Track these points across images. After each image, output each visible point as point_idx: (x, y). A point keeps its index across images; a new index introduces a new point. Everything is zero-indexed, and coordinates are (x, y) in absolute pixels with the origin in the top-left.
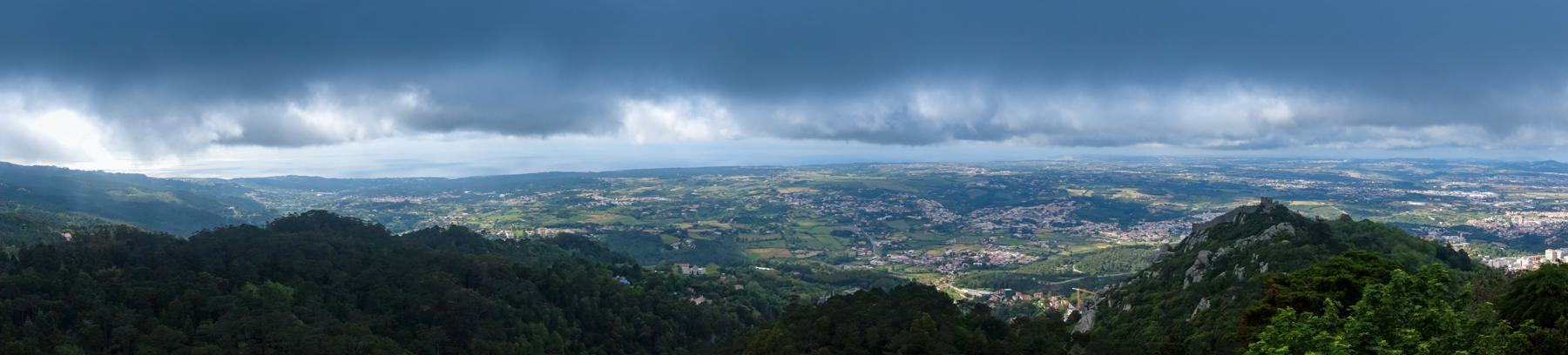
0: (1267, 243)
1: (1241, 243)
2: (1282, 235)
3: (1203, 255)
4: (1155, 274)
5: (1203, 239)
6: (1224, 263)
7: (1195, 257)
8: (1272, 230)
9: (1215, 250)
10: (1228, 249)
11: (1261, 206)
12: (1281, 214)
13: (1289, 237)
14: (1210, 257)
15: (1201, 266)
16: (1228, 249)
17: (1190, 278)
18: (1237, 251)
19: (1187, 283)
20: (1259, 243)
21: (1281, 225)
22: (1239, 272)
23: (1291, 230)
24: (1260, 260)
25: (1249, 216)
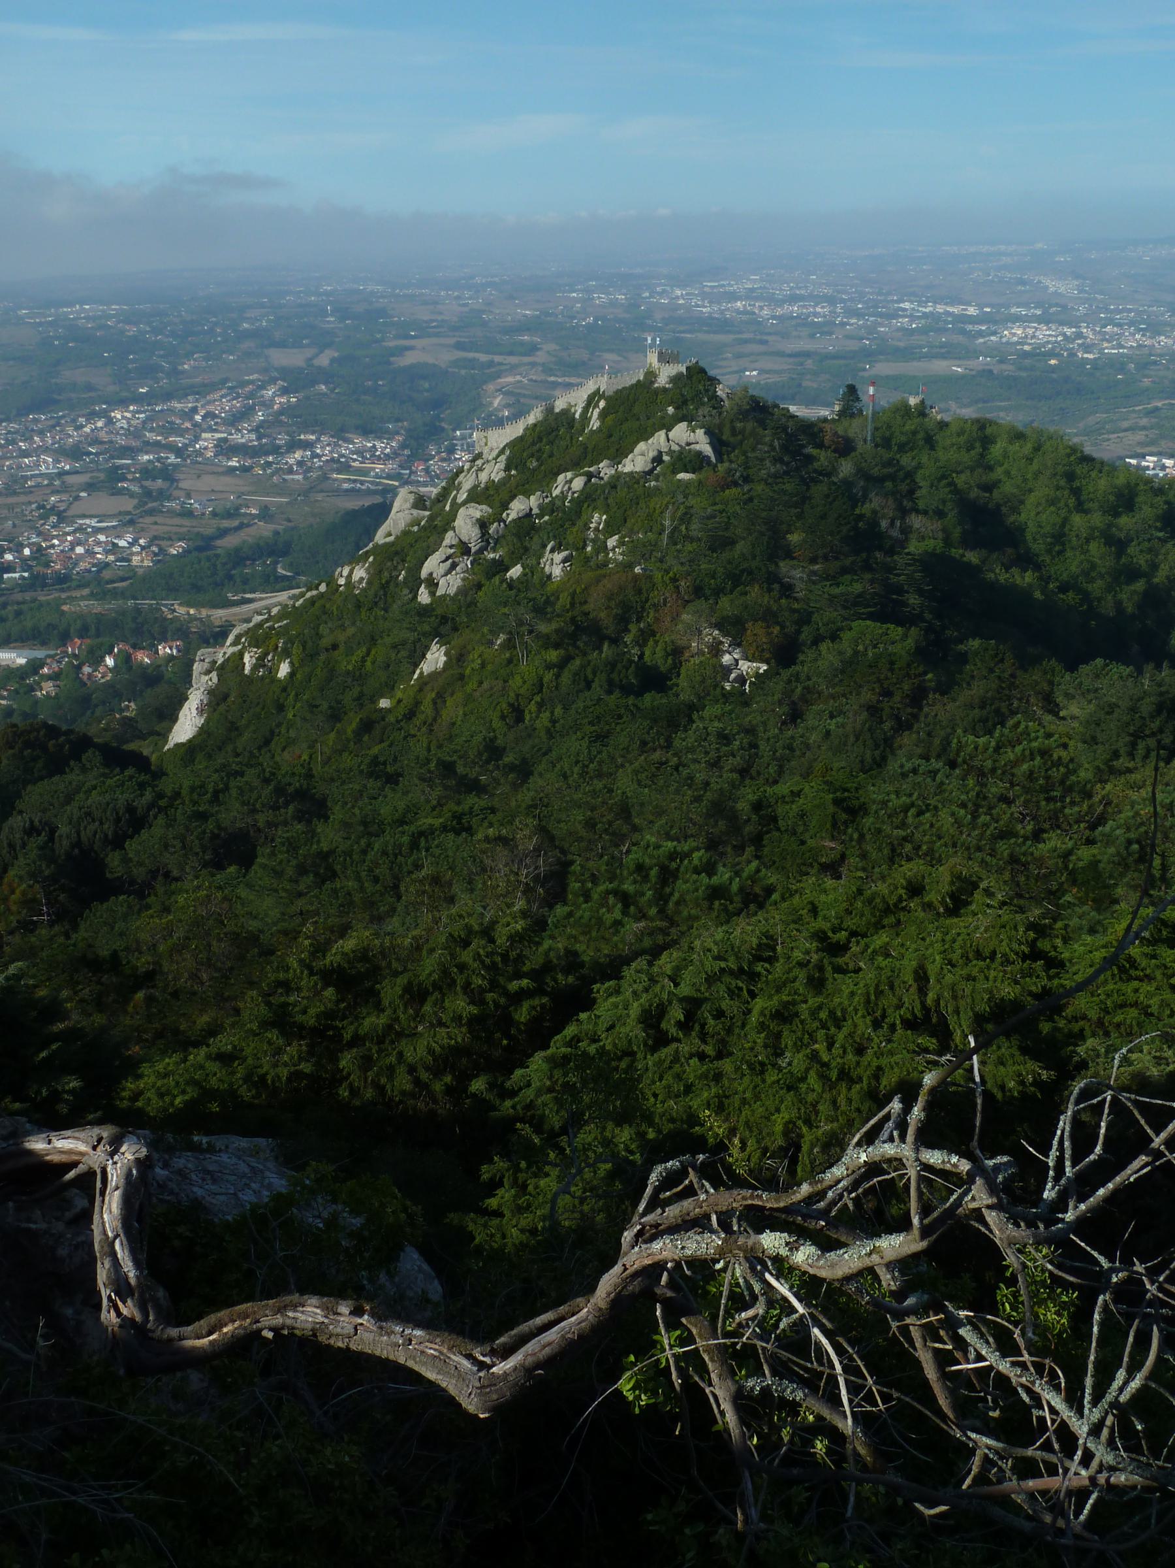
0: (635, 479)
2: (687, 460)
4: (360, 573)
7: (449, 524)
9: (505, 506)
13: (695, 462)
14: (483, 524)
17: (432, 584)
19: (424, 597)
20: (614, 483)
21: (680, 432)
22: (555, 565)
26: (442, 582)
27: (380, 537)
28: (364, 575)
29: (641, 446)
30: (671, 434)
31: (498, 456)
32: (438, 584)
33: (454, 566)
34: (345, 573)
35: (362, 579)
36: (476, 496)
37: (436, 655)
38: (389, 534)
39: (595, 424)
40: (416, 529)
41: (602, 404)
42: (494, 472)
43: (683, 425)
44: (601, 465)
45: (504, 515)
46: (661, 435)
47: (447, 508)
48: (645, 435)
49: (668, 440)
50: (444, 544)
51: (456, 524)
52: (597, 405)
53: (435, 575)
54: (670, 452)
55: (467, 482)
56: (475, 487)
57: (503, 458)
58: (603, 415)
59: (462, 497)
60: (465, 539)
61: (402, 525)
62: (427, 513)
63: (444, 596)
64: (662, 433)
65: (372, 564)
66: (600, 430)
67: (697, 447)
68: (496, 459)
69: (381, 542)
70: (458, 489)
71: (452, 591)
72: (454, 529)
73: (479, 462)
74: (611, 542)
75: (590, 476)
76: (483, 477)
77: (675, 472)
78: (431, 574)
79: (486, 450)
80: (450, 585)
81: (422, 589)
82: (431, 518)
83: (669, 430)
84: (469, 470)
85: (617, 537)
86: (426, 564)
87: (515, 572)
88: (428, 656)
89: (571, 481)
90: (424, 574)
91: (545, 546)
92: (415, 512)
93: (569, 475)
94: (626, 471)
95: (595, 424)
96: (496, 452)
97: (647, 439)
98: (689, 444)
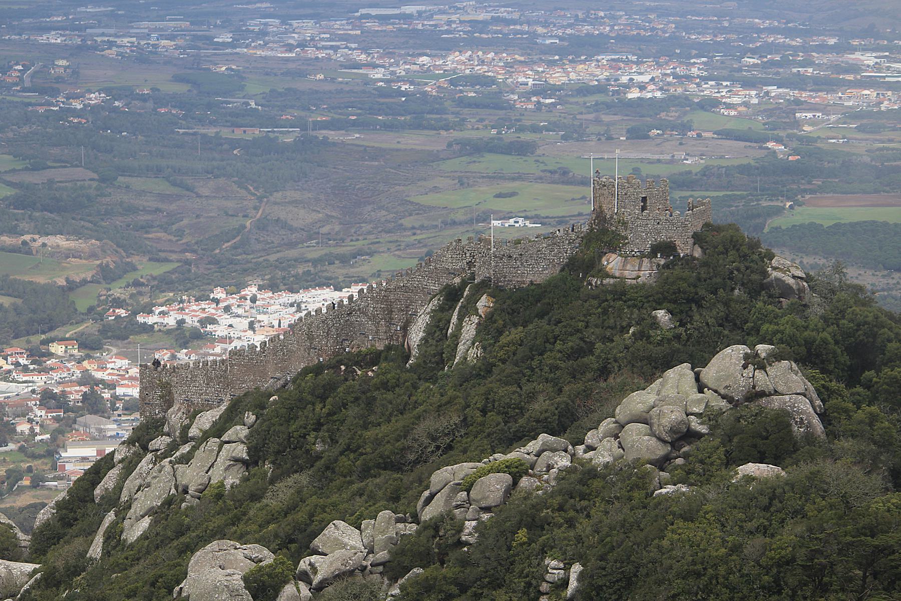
5: (218, 466)
9: (297, 541)
10: (385, 527)
16: (385, 527)
23: (791, 389)
30: (709, 373)
31: (218, 430)
41: (484, 303)
43: (733, 354)
46: (679, 377)
49: (701, 391)
52: (469, 309)
54: (710, 416)
56: (169, 502)
58: (489, 330)
62: (29, 567)
67: (776, 402)
73: (160, 443)
75: (517, 471)
76: (192, 475)
79: (175, 417)
83: (699, 361)
93: (466, 468)
94: (603, 456)
96: (206, 420)
98: (754, 395)
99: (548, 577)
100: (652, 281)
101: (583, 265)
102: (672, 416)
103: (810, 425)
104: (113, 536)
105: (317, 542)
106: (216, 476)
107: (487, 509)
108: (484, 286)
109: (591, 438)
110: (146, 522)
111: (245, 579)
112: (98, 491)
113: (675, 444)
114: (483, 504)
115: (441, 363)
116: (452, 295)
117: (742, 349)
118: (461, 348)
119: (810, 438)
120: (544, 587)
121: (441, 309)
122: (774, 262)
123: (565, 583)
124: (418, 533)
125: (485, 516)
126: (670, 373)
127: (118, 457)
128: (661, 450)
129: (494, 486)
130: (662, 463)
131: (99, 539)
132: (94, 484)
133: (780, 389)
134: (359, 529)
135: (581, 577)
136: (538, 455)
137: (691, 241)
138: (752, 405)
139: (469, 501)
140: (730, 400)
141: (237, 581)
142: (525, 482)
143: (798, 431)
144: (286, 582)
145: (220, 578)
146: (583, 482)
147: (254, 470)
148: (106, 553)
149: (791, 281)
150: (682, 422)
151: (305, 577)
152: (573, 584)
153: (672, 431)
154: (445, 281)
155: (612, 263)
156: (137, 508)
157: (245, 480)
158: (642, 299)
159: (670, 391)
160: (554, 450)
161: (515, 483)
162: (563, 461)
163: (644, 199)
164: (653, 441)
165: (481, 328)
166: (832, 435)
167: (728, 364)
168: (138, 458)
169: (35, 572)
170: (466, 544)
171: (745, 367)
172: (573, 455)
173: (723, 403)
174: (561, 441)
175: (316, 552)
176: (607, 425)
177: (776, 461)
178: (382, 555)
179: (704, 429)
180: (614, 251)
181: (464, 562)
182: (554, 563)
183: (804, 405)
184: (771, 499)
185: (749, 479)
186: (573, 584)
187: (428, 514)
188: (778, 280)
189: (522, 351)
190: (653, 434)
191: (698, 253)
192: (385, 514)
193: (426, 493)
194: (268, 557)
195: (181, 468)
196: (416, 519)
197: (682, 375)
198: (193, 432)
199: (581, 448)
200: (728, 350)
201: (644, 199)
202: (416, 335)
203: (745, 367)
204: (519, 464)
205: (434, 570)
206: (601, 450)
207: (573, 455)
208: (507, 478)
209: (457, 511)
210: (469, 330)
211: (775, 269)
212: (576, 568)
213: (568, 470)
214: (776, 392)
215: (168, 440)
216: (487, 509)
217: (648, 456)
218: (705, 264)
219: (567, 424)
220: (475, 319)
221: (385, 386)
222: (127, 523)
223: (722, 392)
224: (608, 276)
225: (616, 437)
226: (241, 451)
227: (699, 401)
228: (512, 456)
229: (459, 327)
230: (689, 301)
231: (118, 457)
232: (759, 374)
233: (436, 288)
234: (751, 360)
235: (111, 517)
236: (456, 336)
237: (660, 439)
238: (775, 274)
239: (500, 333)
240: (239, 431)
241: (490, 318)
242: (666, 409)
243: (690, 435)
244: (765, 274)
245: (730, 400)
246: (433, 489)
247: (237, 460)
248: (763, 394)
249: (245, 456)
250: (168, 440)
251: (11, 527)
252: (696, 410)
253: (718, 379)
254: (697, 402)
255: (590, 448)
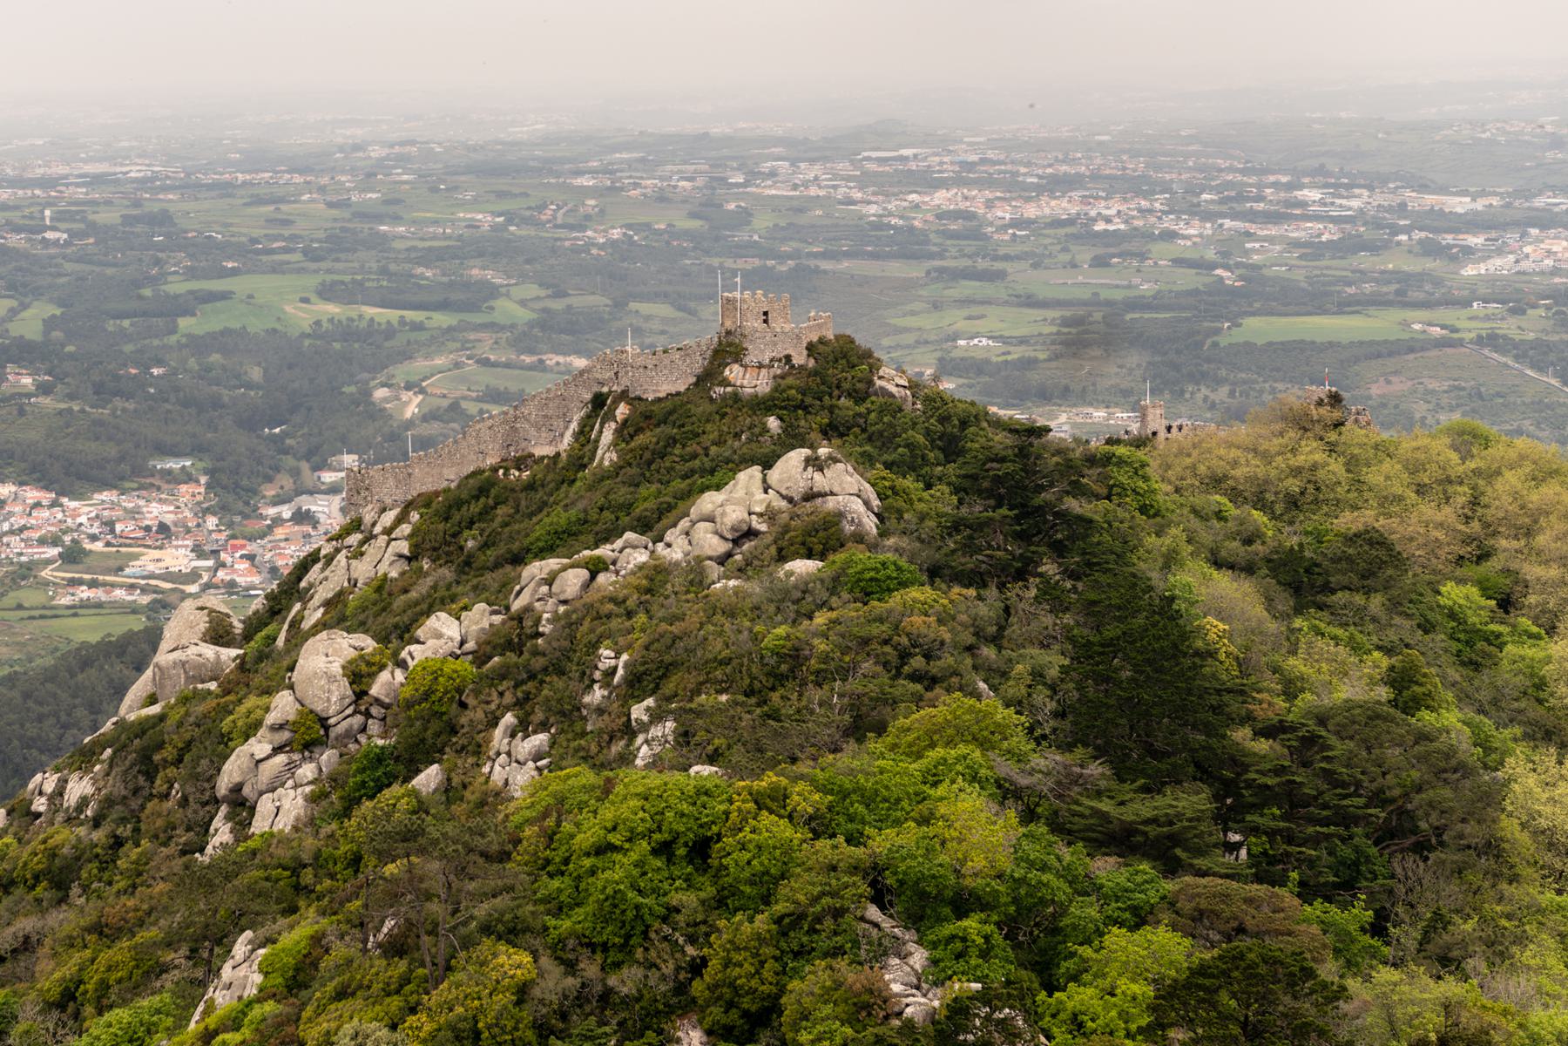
1: (550, 585)
3: (324, 662)
4: (79, 787)
6: (437, 724)
8: (742, 498)
10: (480, 618)
11: (728, 350)
12: (830, 395)
14: (359, 675)
15: (308, 735)
16: (480, 618)
17: (241, 806)
18: (516, 636)
23: (849, 490)
24: (636, 685)
25: (647, 415)
26: (265, 805)
27: (132, 708)
28: (89, 790)
29: (708, 501)
30: (774, 475)
32: (253, 809)
33: (291, 767)
34: (49, 787)
35: (84, 802)
36: (339, 615)
37: (242, 971)
38: (152, 700)
39: (606, 456)
40: (213, 686)
41: (622, 411)
42: (383, 560)
43: (797, 456)
44: (619, 543)
45: (404, 654)
47: (280, 642)
48: (716, 474)
49: (766, 492)
50: (271, 719)
51: (295, 676)
52: (610, 416)
53: (246, 791)
54: (770, 515)
55: (325, 584)
56: (340, 596)
57: (406, 529)
59: (314, 616)
60: (318, 707)
61: (179, 684)
62: (234, 652)
63: (268, 837)
64: (755, 471)
65: (112, 762)
66: (617, 469)
67: (831, 504)
68: (387, 532)
69: (132, 717)
70: (304, 597)
71: (284, 824)
72: (291, 687)
73: (354, 539)
74: (638, 712)
76: (363, 570)
77: (782, 558)
78: (237, 788)
79: (368, 518)
80: (282, 811)
81: (217, 822)
82: (242, 666)
83: (767, 464)
84: (330, 559)
85: (650, 702)
86: (227, 767)
87: (429, 778)
88: (227, 972)
89: (550, 581)
90: (223, 784)
91: (494, 722)
92: (209, 651)
93: (553, 563)
94: (676, 554)
95: (606, 456)
96: (389, 518)
97: (718, 488)
98: (810, 496)
99: (600, 665)
100: (767, 390)
101: (709, 376)
102: (734, 515)
103: (860, 524)
104: (295, 624)
105: (420, 633)
106: (382, 568)
107: (565, 602)
108: (623, 396)
109: (668, 537)
110: (319, 613)
111: (343, 667)
112: (303, 584)
113: (736, 542)
114: (562, 598)
115: (584, 466)
116: (599, 401)
117: (806, 452)
118: (600, 452)
119: (859, 538)
120: (597, 675)
121: (589, 416)
122: (881, 373)
123: (615, 668)
124: (503, 623)
125: (562, 609)
126: (742, 476)
127: (323, 552)
128: (722, 547)
129: (573, 580)
130: (723, 560)
131: (286, 627)
132: (300, 580)
133: (835, 490)
134: (458, 619)
135: (626, 665)
136: (621, 552)
137: (805, 352)
138: (808, 505)
139: (550, 595)
140: (790, 500)
141: (336, 668)
142: (602, 578)
143: (849, 528)
144: (382, 667)
145: (322, 665)
146: (655, 577)
147: (414, 564)
148: (287, 640)
149: (893, 389)
150: (742, 521)
151: (402, 664)
152: (620, 672)
153: (733, 529)
154: (596, 389)
155: (733, 372)
156: (317, 600)
157: (403, 574)
158: (764, 405)
159: (740, 493)
160: (635, 547)
161: (593, 577)
162: (642, 557)
163: (766, 314)
164: (715, 540)
165: (618, 432)
166: (883, 534)
167: (791, 468)
168: (338, 551)
169: (238, 656)
170: (542, 635)
171: (805, 469)
172: (653, 552)
173: (784, 504)
174: (644, 539)
175: (418, 642)
176: (684, 524)
177: (822, 556)
178: (471, 645)
179: (763, 527)
180: (736, 361)
181: (536, 653)
182: (607, 653)
183: (857, 506)
184: (804, 592)
185: (791, 573)
186: (620, 672)
187: (517, 605)
188: (882, 388)
189: (647, 455)
190: (716, 533)
191: (811, 363)
192: (481, 606)
193: (517, 588)
194: (368, 643)
195: (354, 562)
196: (508, 608)
197: (751, 477)
198: (378, 529)
199: (660, 546)
200: (792, 454)
201: (766, 314)
202: (568, 438)
203: (805, 469)
204: (599, 560)
205: (512, 657)
206: (675, 549)
207: (653, 552)
208: (584, 574)
209: (537, 605)
210: (608, 436)
211: (880, 378)
212: (625, 657)
213: (641, 567)
214: (832, 494)
215: (359, 536)
216: (565, 602)
217: (710, 553)
218: (815, 373)
219: (651, 526)
220: (613, 425)
221: (531, 486)
222: (306, 613)
223: (784, 492)
224: (729, 385)
225: (687, 534)
226: (404, 547)
227: (762, 501)
228: (597, 552)
229: (601, 432)
230: (797, 407)
231: (323, 552)
232: (817, 476)
233: (588, 396)
234: (814, 463)
235: (298, 606)
236: (597, 441)
237: (722, 537)
238: (879, 383)
239: (632, 437)
240: (406, 529)
241: (625, 422)
242: (729, 509)
243: (750, 533)
244: (870, 383)
245: (790, 500)
246: (523, 583)
247: (401, 556)
248: (823, 495)
249: (406, 552)
250: (359, 536)
251: (228, 616)
252: (758, 509)
253: (780, 481)
254: (760, 501)
255: (669, 545)
